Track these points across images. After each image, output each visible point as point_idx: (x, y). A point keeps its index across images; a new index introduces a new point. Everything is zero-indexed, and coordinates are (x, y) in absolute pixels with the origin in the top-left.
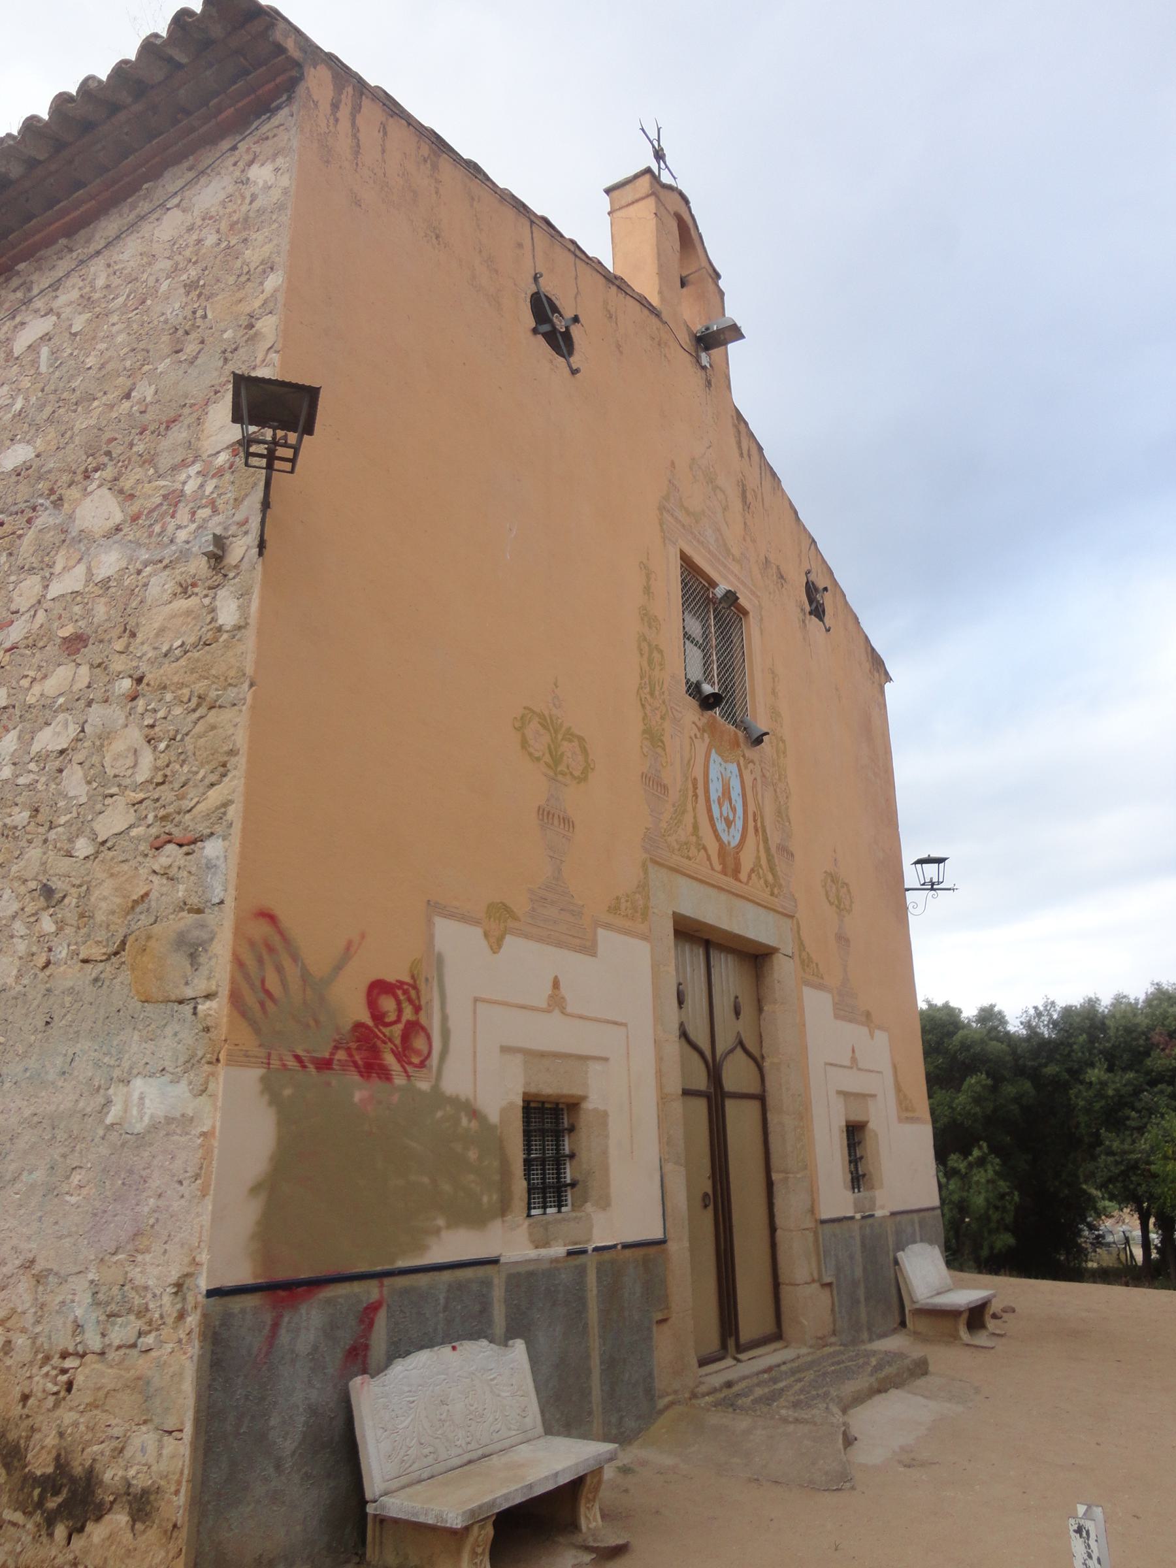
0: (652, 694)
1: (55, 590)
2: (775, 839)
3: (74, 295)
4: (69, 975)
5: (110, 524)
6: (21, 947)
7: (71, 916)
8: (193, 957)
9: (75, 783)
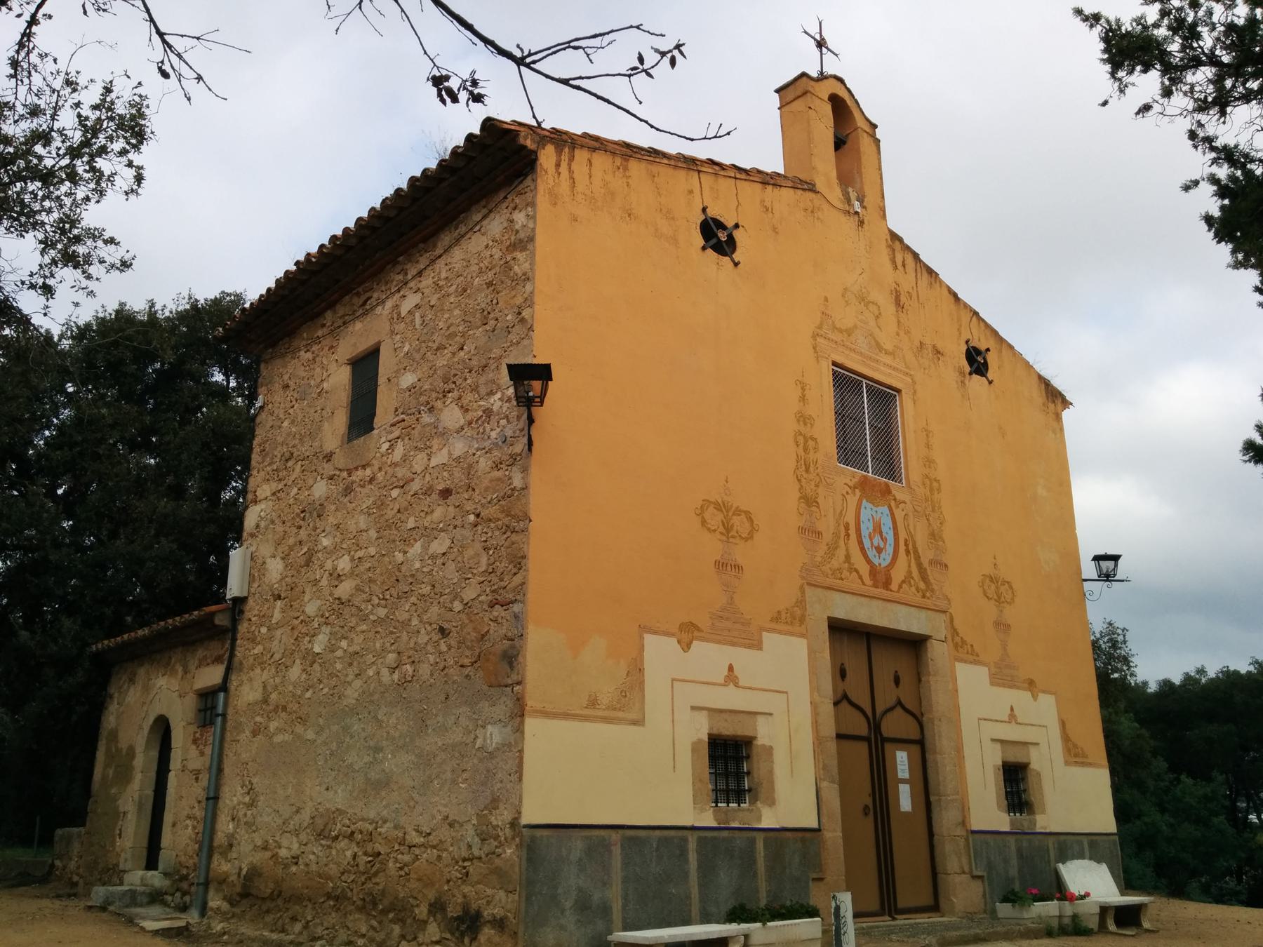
0: (807, 471)
1: (433, 462)
2: (927, 555)
3: (430, 281)
4: (454, 672)
5: (457, 426)
6: (432, 658)
7: (453, 643)
8: (511, 664)
9: (451, 572)
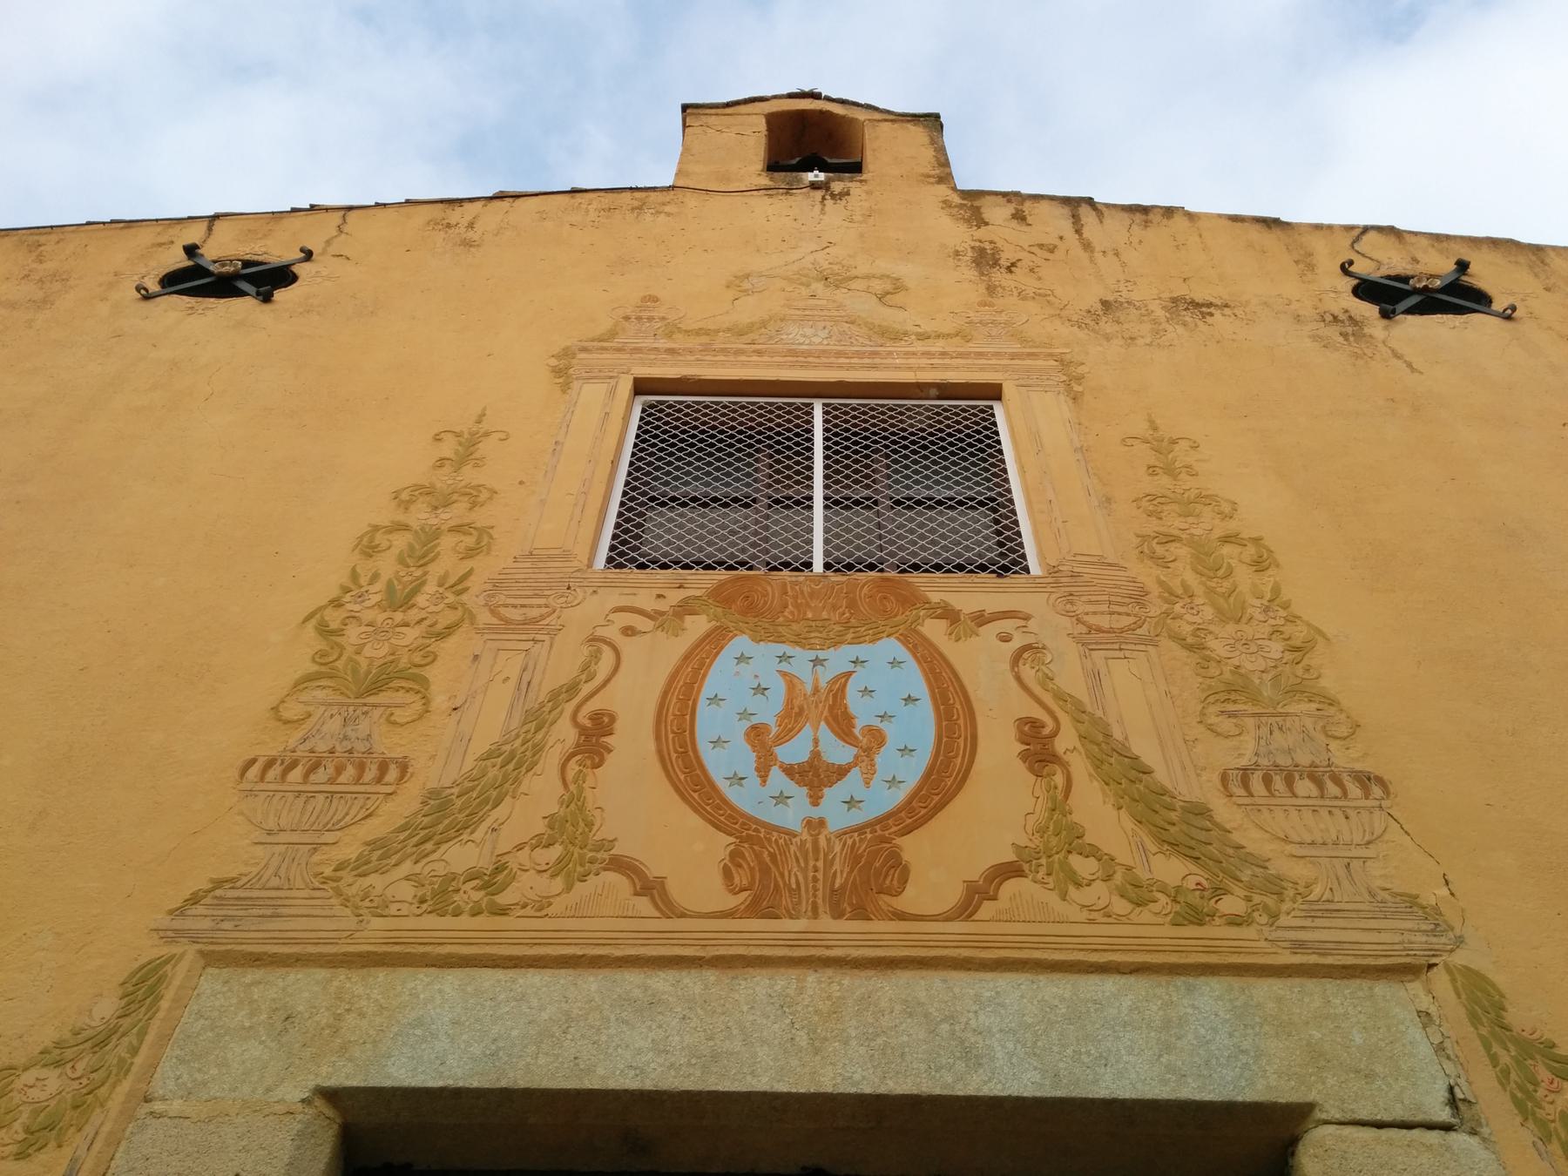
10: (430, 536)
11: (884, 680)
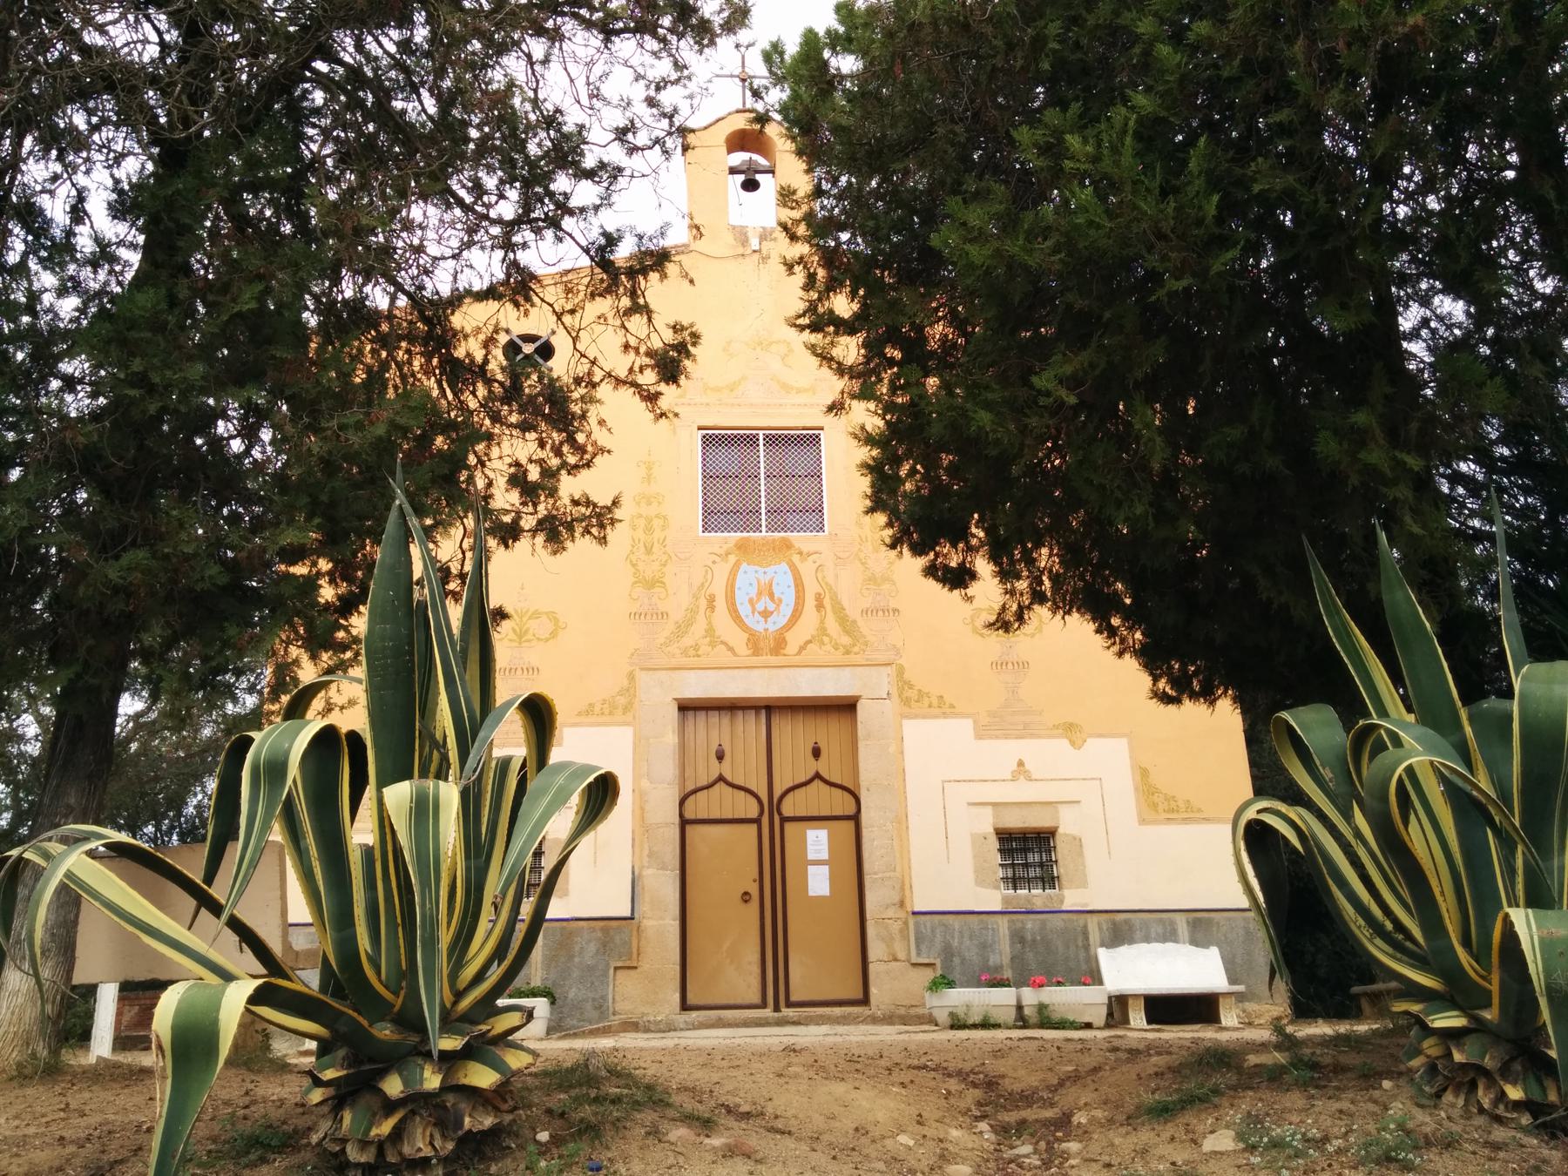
0: (649, 551)
10: (649, 520)
11: (781, 577)
